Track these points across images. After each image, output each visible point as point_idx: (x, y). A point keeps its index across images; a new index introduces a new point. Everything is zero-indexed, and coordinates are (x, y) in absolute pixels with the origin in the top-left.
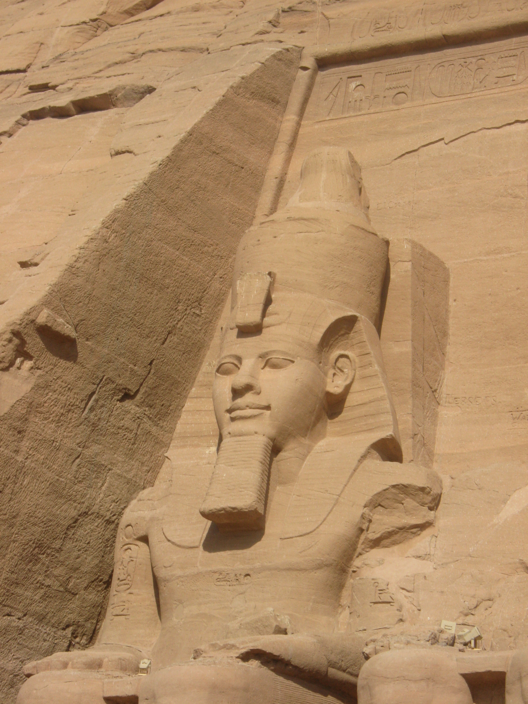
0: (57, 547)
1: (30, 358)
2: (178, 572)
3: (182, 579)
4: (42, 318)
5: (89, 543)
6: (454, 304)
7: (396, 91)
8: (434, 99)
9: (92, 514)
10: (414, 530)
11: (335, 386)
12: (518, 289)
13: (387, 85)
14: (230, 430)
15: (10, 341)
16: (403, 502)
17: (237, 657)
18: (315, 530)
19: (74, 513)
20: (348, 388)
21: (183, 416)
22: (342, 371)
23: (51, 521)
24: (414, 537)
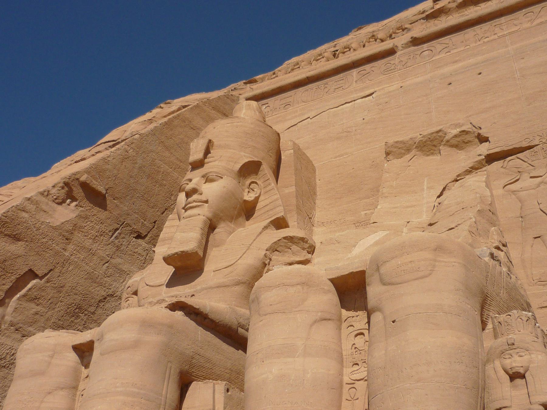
0: (92, 311)
1: (76, 200)
4: (83, 178)
7: (284, 105)
8: (304, 104)
9: (116, 296)
11: (249, 197)
13: (281, 103)
14: (184, 216)
15: (63, 188)
17: (166, 307)
19: (104, 294)
20: (257, 199)
21: (164, 229)
22: (253, 191)
23: (87, 294)
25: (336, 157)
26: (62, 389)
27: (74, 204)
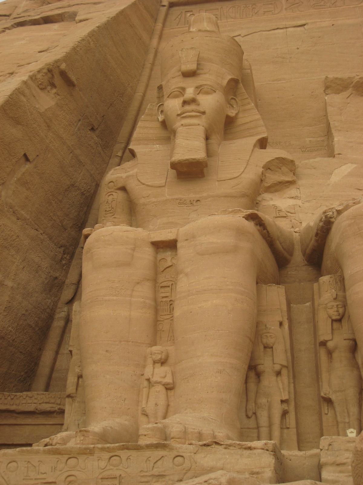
0: (61, 199)
2: (154, 200)
3: (156, 203)
4: (63, 66)
5: (74, 202)
6: (259, 101)
8: (233, 20)
10: (287, 184)
11: (232, 113)
12: (293, 95)
15: (46, 74)
16: (281, 168)
17: (243, 217)
18: (239, 176)
20: (237, 114)
24: (286, 188)
25: (273, 81)
26: (148, 280)
27: (54, 91)
